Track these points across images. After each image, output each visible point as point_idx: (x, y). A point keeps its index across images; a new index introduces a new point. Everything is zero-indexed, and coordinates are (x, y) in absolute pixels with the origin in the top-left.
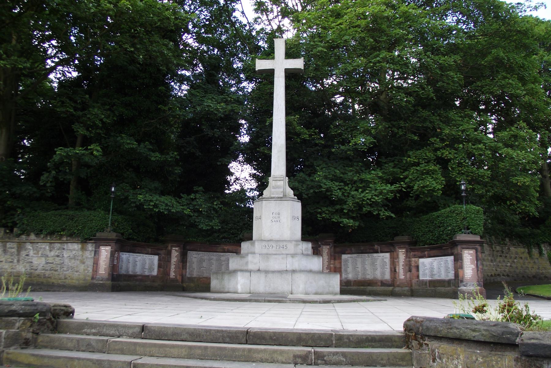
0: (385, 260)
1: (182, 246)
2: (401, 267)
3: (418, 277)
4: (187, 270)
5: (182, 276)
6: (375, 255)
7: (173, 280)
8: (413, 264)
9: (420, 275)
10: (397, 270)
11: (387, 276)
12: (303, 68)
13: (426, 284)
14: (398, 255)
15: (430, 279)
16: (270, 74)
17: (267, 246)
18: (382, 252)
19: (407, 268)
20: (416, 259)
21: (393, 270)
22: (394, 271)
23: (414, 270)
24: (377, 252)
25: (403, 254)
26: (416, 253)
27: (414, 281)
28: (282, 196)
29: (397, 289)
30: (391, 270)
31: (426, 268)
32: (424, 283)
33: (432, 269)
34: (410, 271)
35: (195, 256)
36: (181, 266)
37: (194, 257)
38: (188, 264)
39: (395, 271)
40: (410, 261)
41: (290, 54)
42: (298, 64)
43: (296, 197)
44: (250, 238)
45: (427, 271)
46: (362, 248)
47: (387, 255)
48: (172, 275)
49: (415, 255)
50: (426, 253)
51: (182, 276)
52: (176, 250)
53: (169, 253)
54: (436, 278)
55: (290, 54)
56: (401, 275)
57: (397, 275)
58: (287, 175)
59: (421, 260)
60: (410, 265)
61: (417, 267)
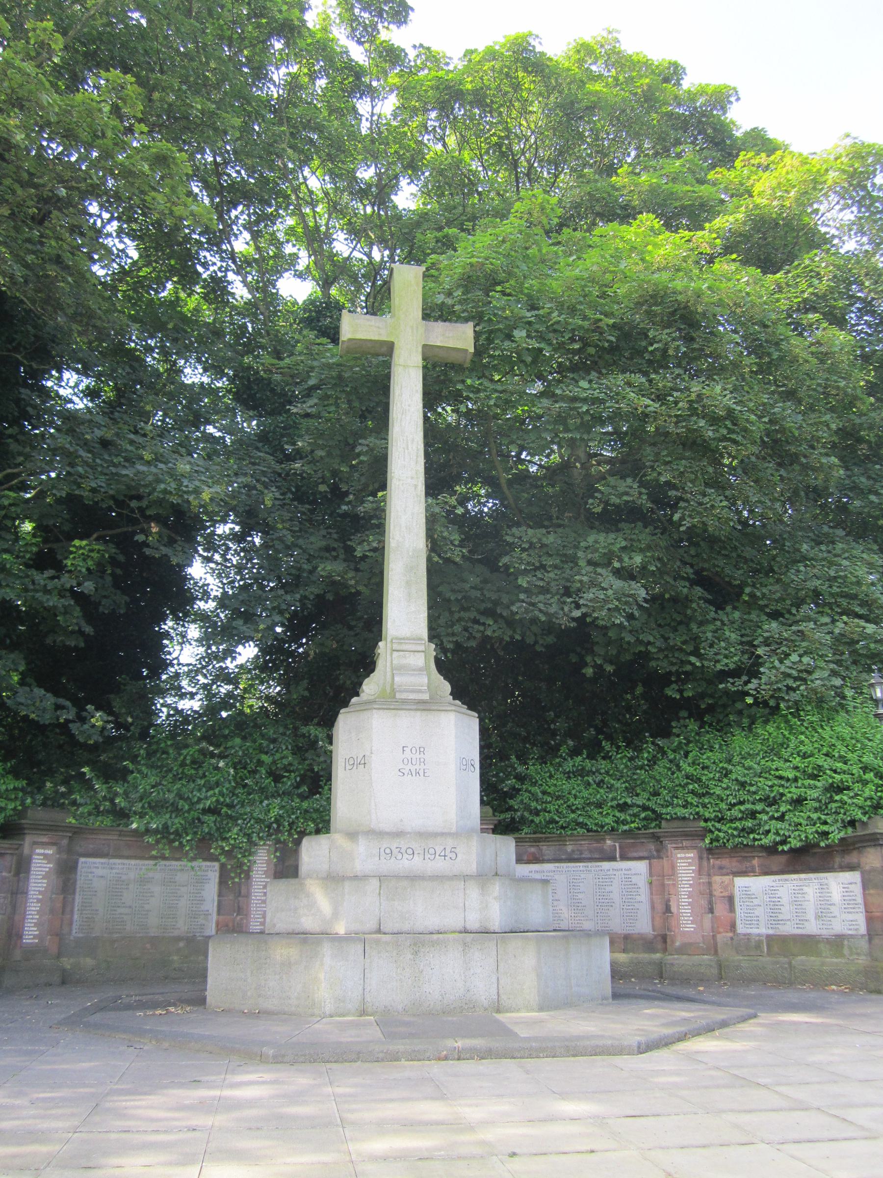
0: (634, 879)
1: (65, 842)
2: (685, 900)
3: (733, 926)
4: (76, 917)
5: (59, 935)
6: (606, 865)
7: (31, 952)
8: (718, 892)
9: (738, 922)
10: (674, 909)
11: (643, 925)
12: (472, 350)
13: (758, 946)
14: (673, 867)
15: (771, 932)
16: (381, 356)
17: (395, 851)
18: (624, 858)
19: (704, 902)
20: (726, 879)
21: (660, 907)
22: (664, 910)
23: (721, 909)
24: (612, 859)
25: (690, 864)
26: (725, 862)
27: (723, 937)
28: (426, 697)
29: (679, 962)
30: (653, 908)
31: (756, 902)
32: (750, 945)
33: (775, 906)
34: (711, 911)
35: (100, 872)
36: (59, 905)
37: (97, 872)
38: (78, 899)
39: (668, 909)
40: (710, 884)
41: (433, 312)
42: (459, 338)
43: (458, 702)
44: (322, 824)
45: (759, 912)
46: (569, 848)
47: (641, 867)
48: (31, 933)
49: (721, 868)
50: (755, 862)
51: (59, 935)
52: (46, 856)
53: (22, 867)
54: (789, 929)
55: (433, 312)
56: (687, 922)
57: (673, 923)
58: (431, 638)
59: (740, 882)
60: (711, 894)
61: (731, 900)
